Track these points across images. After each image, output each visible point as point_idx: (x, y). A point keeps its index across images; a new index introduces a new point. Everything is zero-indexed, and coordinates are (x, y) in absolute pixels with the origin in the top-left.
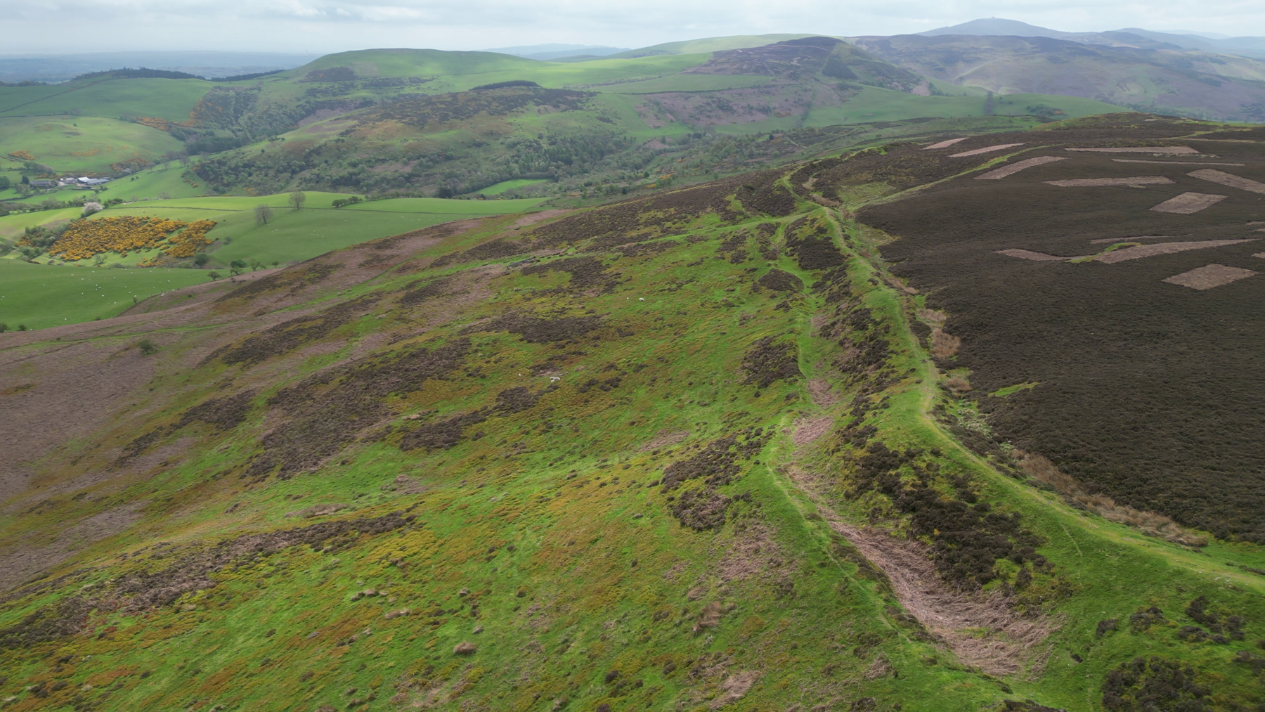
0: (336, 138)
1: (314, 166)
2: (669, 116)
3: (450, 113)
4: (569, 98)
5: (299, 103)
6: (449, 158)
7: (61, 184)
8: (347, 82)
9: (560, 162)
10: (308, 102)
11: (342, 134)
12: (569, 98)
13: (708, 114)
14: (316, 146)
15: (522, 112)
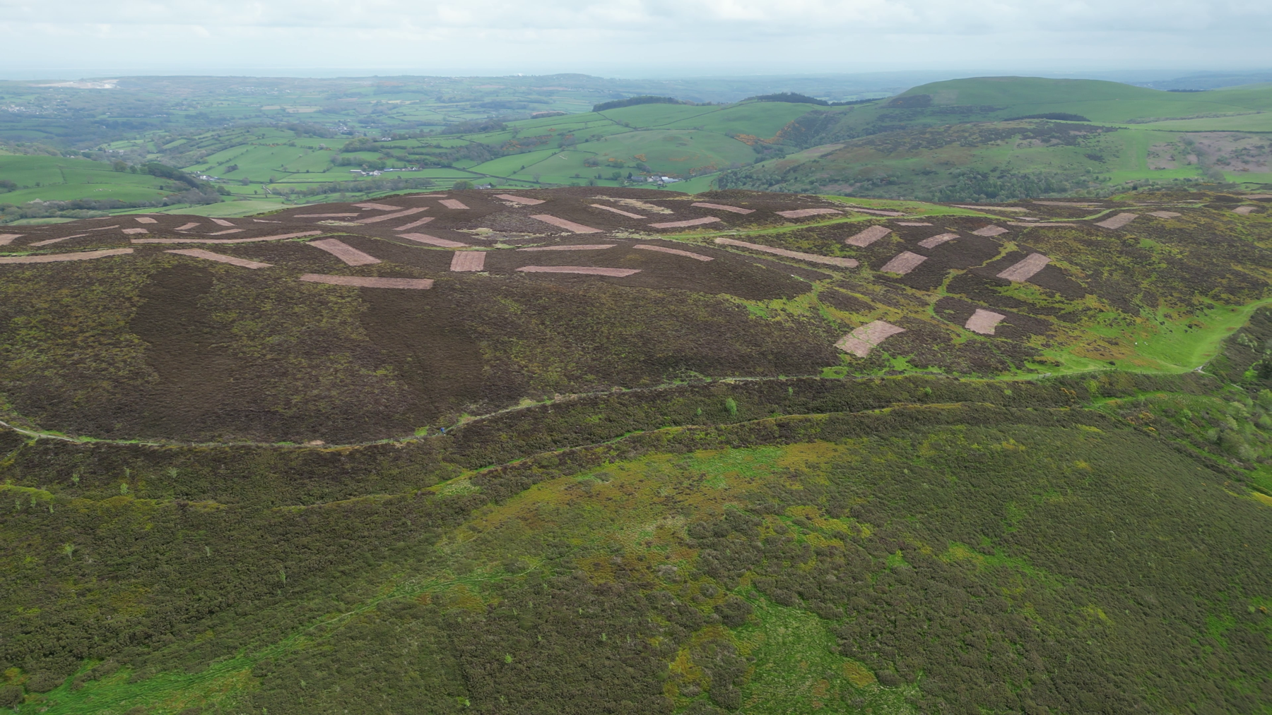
0: (812, 160)
1: (786, 181)
2: (1193, 158)
3: (924, 143)
4: (1072, 133)
5: (867, 127)
6: (891, 183)
7: (650, 180)
8: (919, 109)
9: (982, 195)
10: (874, 126)
11: (822, 156)
12: (1072, 133)
13: (1246, 158)
14: (796, 165)
15: (998, 145)
